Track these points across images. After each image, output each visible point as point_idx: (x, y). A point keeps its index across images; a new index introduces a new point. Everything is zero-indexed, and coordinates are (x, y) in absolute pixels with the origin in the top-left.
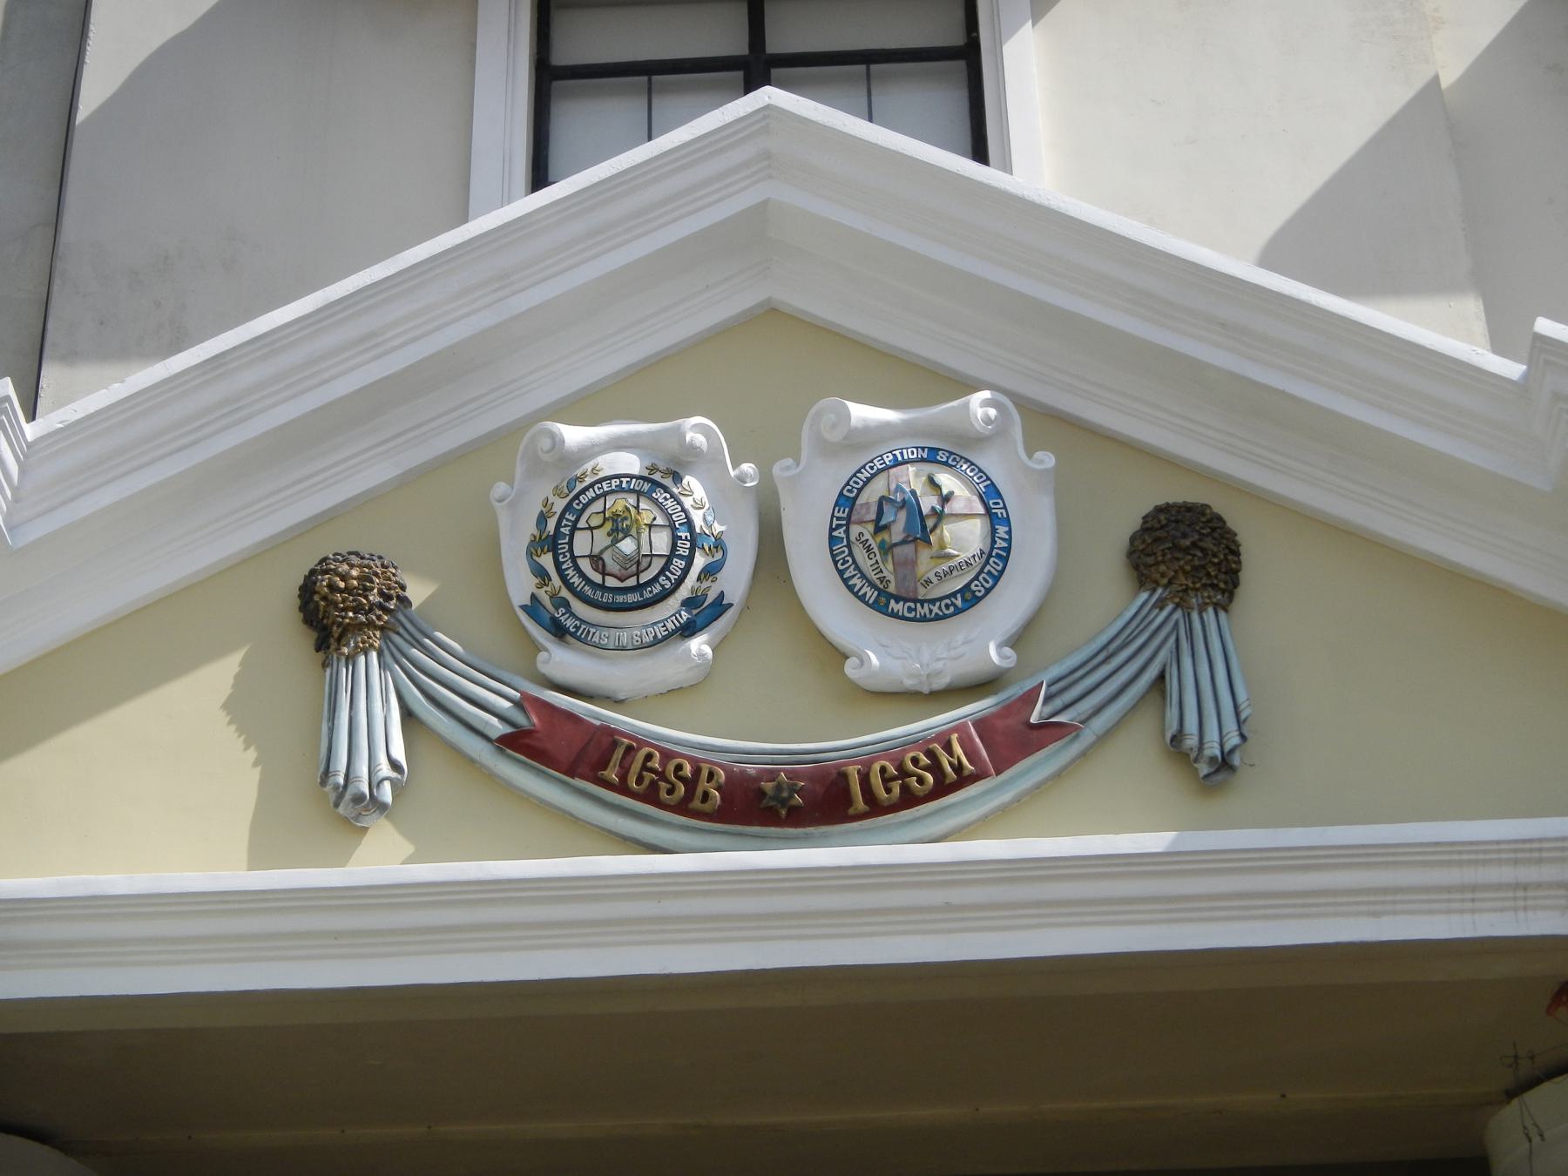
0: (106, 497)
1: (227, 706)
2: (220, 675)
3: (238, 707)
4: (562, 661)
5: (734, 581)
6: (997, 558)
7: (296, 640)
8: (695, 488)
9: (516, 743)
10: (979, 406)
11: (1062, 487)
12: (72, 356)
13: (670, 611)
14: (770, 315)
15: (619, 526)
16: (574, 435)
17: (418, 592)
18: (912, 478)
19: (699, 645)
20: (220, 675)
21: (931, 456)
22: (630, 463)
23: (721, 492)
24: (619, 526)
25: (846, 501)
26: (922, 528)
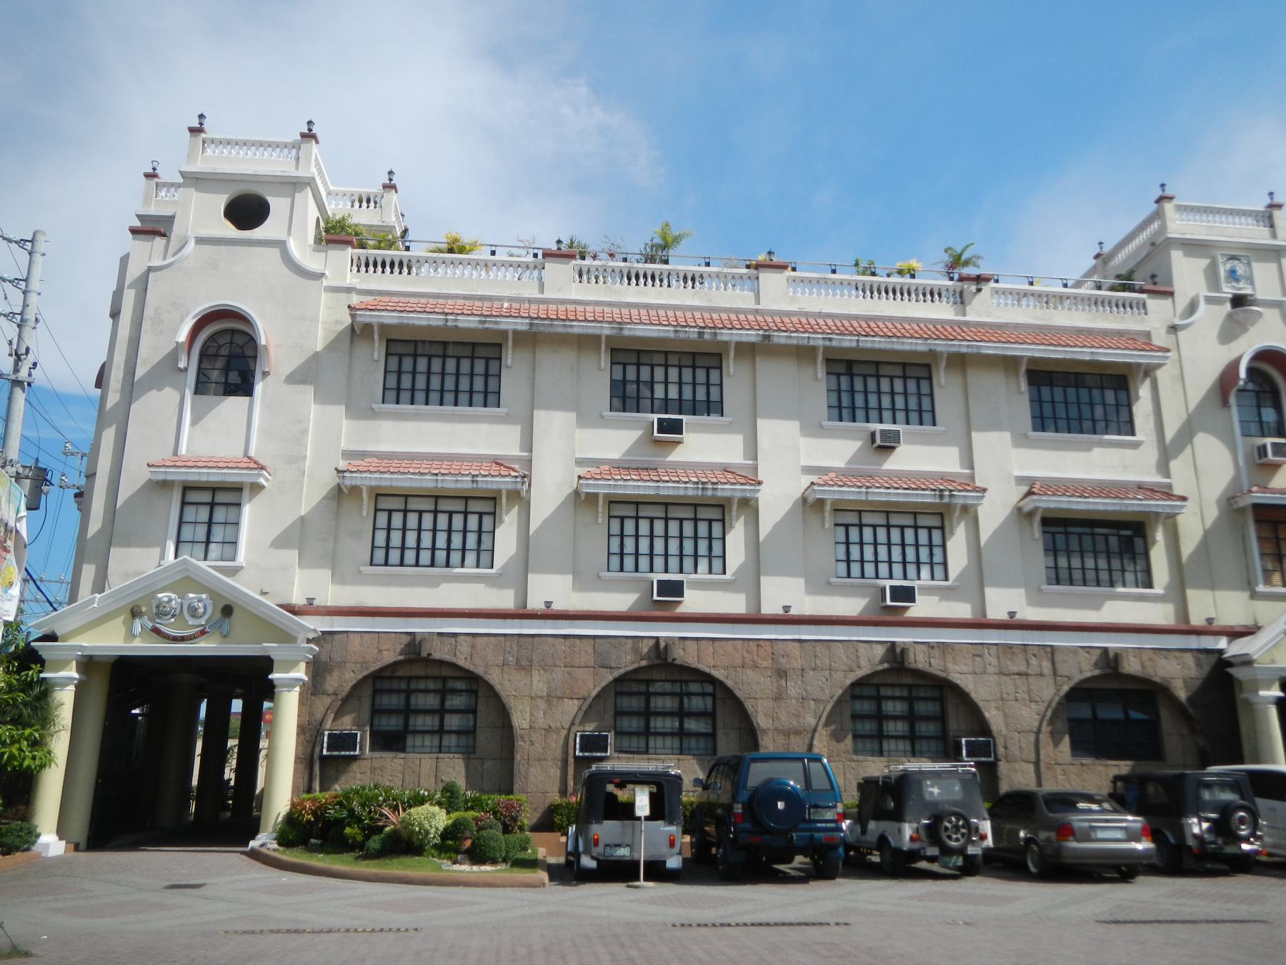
0: (108, 602)
1: (123, 623)
2: (122, 618)
3: (124, 622)
4: (158, 621)
5: (178, 612)
6: (204, 613)
7: (131, 616)
8: (174, 602)
9: (151, 630)
10: (204, 596)
11: (214, 604)
12: (115, 546)
13: (170, 616)
14: (187, 578)
15: (164, 607)
16: (160, 595)
17: (144, 609)
18: (196, 604)
19: (173, 620)
20: (122, 618)
21: (199, 601)
22: (166, 599)
23: (177, 602)
24: (164, 607)
25: (189, 606)
26: (196, 610)
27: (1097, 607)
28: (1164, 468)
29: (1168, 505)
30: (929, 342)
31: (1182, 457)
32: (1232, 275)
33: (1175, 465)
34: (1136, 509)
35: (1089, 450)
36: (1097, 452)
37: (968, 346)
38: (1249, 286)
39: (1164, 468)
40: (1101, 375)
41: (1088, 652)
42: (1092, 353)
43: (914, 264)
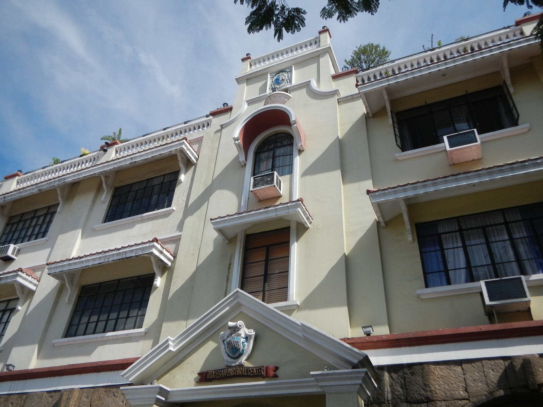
27: (89, 353)
28: (180, 227)
29: (140, 249)
30: (39, 185)
31: (198, 212)
32: (277, 82)
33: (189, 221)
34: (115, 258)
35: (132, 227)
36: (138, 226)
37: (59, 180)
38: (289, 83)
39: (180, 227)
40: (164, 175)
41: (52, 397)
42: (132, 158)
43: (83, 150)
